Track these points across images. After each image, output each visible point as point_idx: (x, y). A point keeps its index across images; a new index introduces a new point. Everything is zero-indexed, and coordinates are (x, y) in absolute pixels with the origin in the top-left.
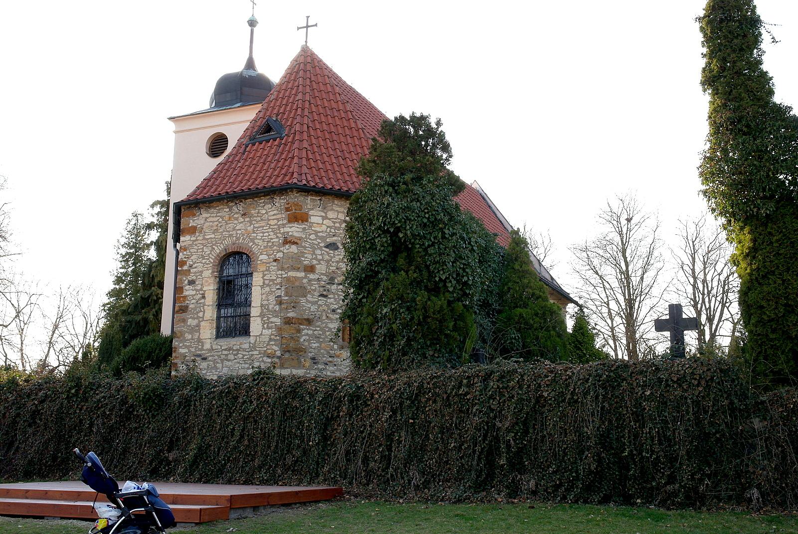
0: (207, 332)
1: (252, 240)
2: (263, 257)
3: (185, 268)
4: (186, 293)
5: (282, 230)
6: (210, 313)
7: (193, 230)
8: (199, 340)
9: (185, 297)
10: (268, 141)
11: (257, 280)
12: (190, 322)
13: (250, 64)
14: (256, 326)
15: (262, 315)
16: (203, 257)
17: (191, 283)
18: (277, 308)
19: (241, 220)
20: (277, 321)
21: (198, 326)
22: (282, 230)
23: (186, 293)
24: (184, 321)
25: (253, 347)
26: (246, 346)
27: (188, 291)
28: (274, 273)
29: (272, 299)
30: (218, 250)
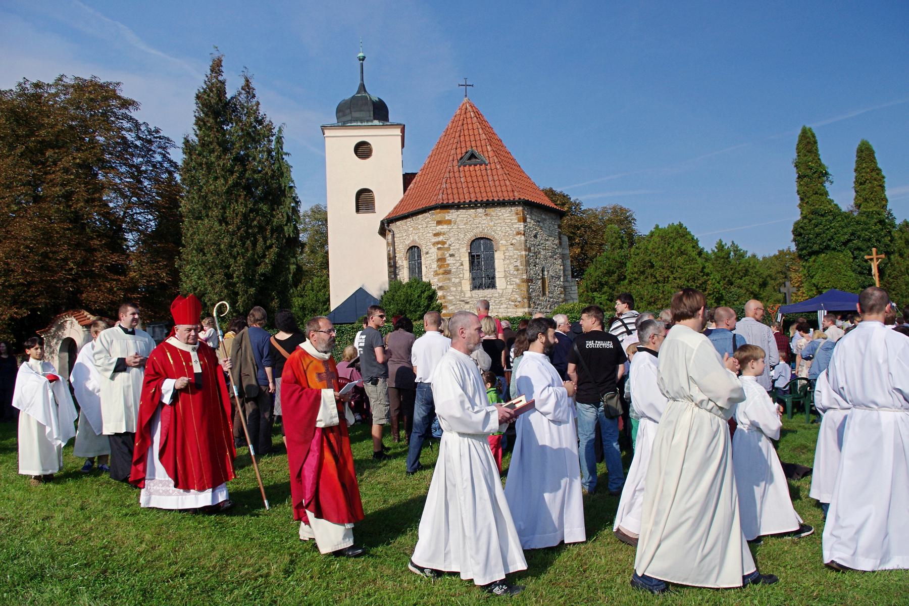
0: (467, 285)
1: (494, 231)
2: (503, 242)
3: (446, 246)
4: (448, 262)
5: (515, 226)
6: (467, 275)
7: (449, 222)
8: (462, 291)
9: (448, 265)
10: (475, 165)
11: (498, 255)
12: (453, 280)
13: (362, 87)
14: (500, 282)
15: (506, 277)
16: (458, 239)
17: (452, 255)
18: (515, 273)
19: (484, 217)
20: (518, 281)
21: (460, 283)
22: (515, 226)
23: (448, 262)
24: (449, 279)
25: (502, 296)
26: (497, 295)
27: (450, 261)
28: (511, 252)
29: (511, 267)
30: (470, 236)
